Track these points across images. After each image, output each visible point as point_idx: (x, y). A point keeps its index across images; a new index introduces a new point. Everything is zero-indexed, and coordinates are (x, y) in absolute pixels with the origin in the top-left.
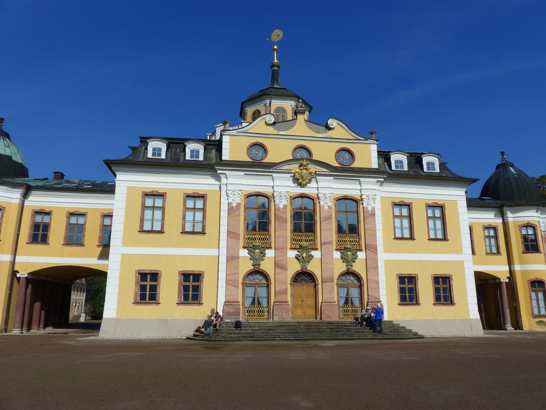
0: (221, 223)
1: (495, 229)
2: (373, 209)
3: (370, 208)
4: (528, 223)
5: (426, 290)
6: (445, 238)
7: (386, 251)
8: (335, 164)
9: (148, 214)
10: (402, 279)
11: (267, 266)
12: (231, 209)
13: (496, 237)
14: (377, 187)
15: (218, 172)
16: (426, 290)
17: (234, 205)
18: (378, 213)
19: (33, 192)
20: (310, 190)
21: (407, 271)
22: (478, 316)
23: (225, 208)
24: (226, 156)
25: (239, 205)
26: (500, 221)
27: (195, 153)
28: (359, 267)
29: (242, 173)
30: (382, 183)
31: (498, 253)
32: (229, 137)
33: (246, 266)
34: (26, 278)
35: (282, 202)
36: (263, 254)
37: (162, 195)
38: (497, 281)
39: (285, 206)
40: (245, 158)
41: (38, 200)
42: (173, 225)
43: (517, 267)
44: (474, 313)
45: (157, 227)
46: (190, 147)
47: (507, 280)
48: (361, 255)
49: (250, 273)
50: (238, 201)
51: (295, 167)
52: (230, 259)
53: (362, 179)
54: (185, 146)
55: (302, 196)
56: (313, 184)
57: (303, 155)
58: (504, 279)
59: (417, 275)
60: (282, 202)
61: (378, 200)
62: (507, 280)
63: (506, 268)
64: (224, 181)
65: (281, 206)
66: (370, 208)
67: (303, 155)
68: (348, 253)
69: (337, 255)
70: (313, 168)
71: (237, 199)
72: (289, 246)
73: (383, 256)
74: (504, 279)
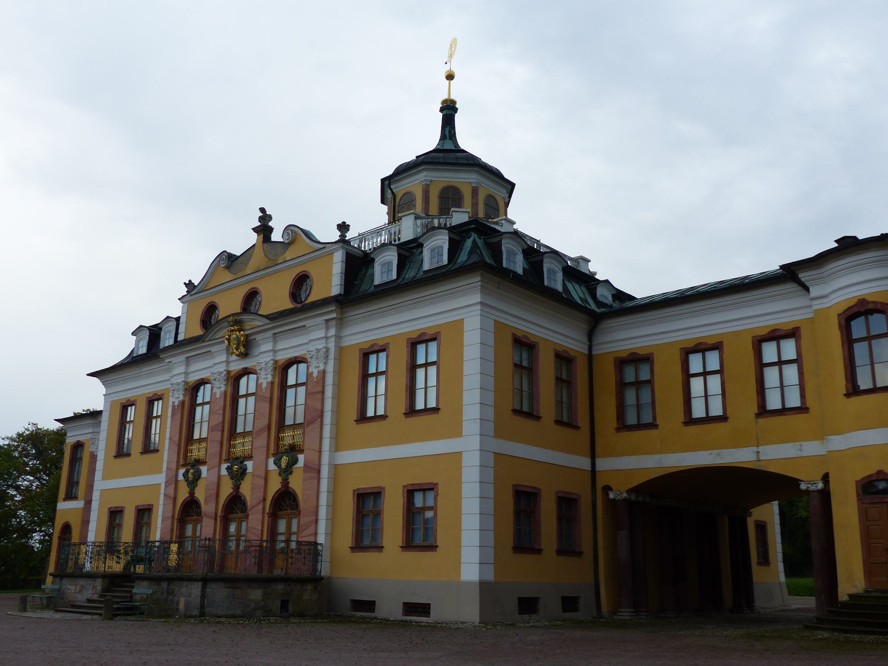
4: (862, 301)
15: (167, 361)
17: (176, 404)
28: (296, 483)
30: (341, 323)
33: (183, 494)
36: (198, 476)
47: (820, 486)
50: (181, 397)
53: (308, 323)
56: (256, 351)
59: (383, 488)
62: (820, 486)
69: (272, 466)
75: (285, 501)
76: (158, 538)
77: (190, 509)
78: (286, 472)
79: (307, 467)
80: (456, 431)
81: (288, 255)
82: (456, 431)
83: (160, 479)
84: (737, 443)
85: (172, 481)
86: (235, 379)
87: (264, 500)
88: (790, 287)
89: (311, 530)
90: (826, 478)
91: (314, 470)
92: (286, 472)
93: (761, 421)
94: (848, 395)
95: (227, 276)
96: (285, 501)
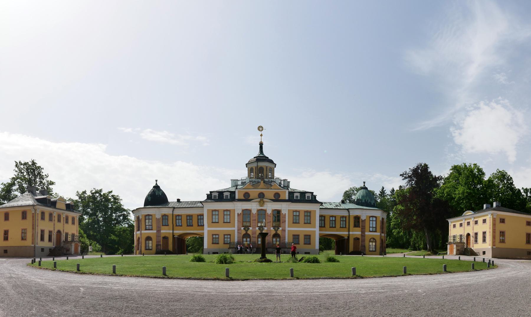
1: (346, 217)
6: (310, 223)
7: (288, 227)
8: (274, 198)
9: (214, 216)
11: (249, 232)
13: (346, 221)
23: (236, 215)
24: (237, 197)
28: (279, 232)
31: (346, 227)
33: (244, 232)
35: (254, 212)
42: (221, 221)
43: (351, 233)
44: (317, 246)
45: (217, 221)
46: (225, 194)
48: (281, 229)
49: (244, 235)
51: (259, 200)
52: (238, 230)
55: (262, 210)
57: (261, 196)
60: (254, 212)
67: (261, 196)
68: (276, 227)
69: (272, 228)
70: (265, 200)
73: (287, 229)
74: (346, 238)
75: (276, 235)
76: (236, 240)
77: (246, 235)
78: (276, 231)
80: (315, 227)
81: (272, 188)
82: (315, 227)
83: (236, 229)
84: (337, 231)
85: (239, 229)
86: (258, 211)
88: (346, 211)
90: (348, 237)
91: (284, 230)
92: (276, 231)
95: (252, 188)
96: (276, 235)
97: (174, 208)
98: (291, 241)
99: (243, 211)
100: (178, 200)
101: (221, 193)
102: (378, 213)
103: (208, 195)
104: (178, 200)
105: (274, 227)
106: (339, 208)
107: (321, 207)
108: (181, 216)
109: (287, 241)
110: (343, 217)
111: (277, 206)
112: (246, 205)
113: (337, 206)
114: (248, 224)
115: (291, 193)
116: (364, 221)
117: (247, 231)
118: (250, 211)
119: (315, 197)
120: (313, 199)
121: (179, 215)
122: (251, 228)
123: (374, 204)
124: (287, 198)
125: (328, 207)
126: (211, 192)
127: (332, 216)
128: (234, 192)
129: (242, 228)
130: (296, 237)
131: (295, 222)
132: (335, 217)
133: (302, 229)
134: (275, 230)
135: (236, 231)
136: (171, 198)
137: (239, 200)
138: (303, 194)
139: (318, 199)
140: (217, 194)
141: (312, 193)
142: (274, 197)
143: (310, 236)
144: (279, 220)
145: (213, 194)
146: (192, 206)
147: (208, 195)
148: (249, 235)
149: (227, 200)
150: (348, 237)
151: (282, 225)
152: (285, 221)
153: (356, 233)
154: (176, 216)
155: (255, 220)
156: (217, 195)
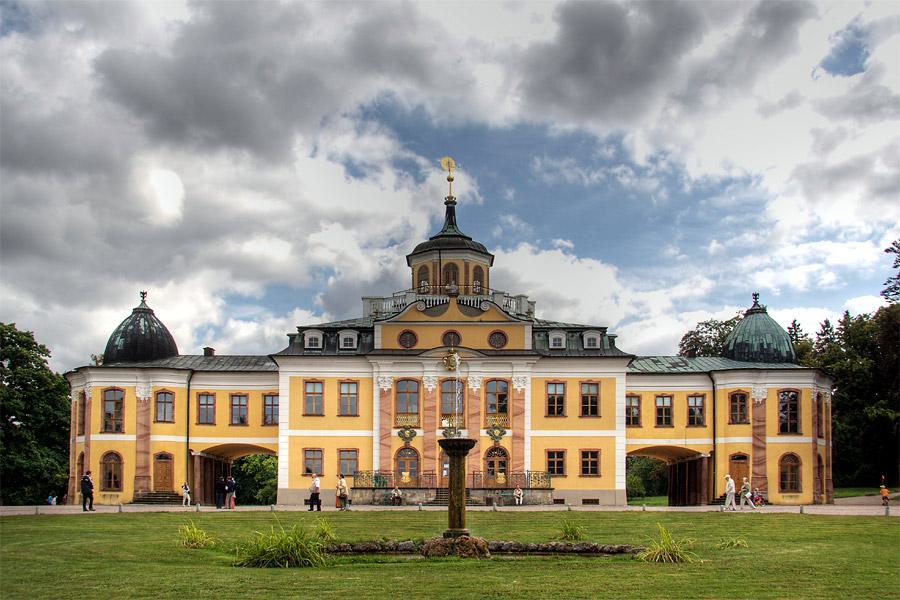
0: (372, 405)
1: (703, 396)
2: (523, 392)
3: (519, 390)
5: (573, 463)
10: (550, 454)
11: (416, 443)
12: (383, 394)
14: (528, 369)
16: (573, 463)
18: (528, 394)
19: (196, 376)
20: (458, 374)
21: (556, 446)
22: (624, 488)
23: (376, 394)
24: (378, 345)
25: (390, 390)
26: (711, 389)
27: (349, 341)
29: (391, 362)
32: (380, 327)
33: (399, 444)
34: (201, 457)
36: (413, 435)
37: (321, 382)
38: (697, 457)
39: (434, 390)
40: (398, 347)
41: (201, 385)
43: (720, 440)
44: (621, 484)
46: (343, 335)
48: (509, 433)
52: (382, 438)
53: (513, 362)
54: (338, 335)
57: (451, 339)
58: (706, 454)
61: (529, 380)
63: (711, 441)
64: (376, 369)
65: (430, 390)
66: (519, 390)
67: (451, 339)
69: (483, 433)
71: (388, 386)
72: (438, 426)
73: (529, 433)
74: (706, 454)
79: (515, 437)
80: (612, 427)
81: (483, 317)
83: (376, 434)
85: (385, 436)
87: (479, 452)
88: (706, 377)
89: (520, 468)
90: (713, 453)
91: (519, 438)
92: (496, 439)
93: (688, 429)
94: (729, 424)
95: (425, 317)
97: (193, 372)
98: (543, 467)
99: (398, 382)
100: (209, 352)
101: (330, 332)
102: (806, 385)
103: (292, 337)
104: (209, 352)
105: (490, 430)
106: (682, 370)
107: (629, 370)
108: (213, 395)
109: (527, 467)
110: (695, 396)
111: (499, 371)
112: (410, 371)
113: (675, 365)
114: (412, 421)
115: (543, 330)
116: (761, 405)
117: (407, 440)
118: (418, 382)
119: (612, 339)
120: (607, 347)
121: (207, 395)
122: (419, 432)
123: (789, 353)
124: (528, 345)
125: (651, 370)
126: (301, 329)
127: (662, 396)
128: (371, 331)
129: (395, 432)
130: (556, 463)
131: (555, 407)
132: (671, 397)
133: (573, 434)
134: (493, 437)
135: (376, 440)
136: (186, 344)
137: (387, 353)
138: (576, 331)
139: (623, 346)
140: (319, 335)
141: (603, 330)
142: (490, 343)
143: (595, 454)
144: (503, 409)
145: (308, 335)
146: (248, 368)
147: (292, 337)
148: (415, 451)
149: (348, 355)
150: (713, 453)
151: (513, 421)
152: (523, 412)
153: (739, 439)
154: (200, 395)
155: (433, 408)
156: (321, 339)
